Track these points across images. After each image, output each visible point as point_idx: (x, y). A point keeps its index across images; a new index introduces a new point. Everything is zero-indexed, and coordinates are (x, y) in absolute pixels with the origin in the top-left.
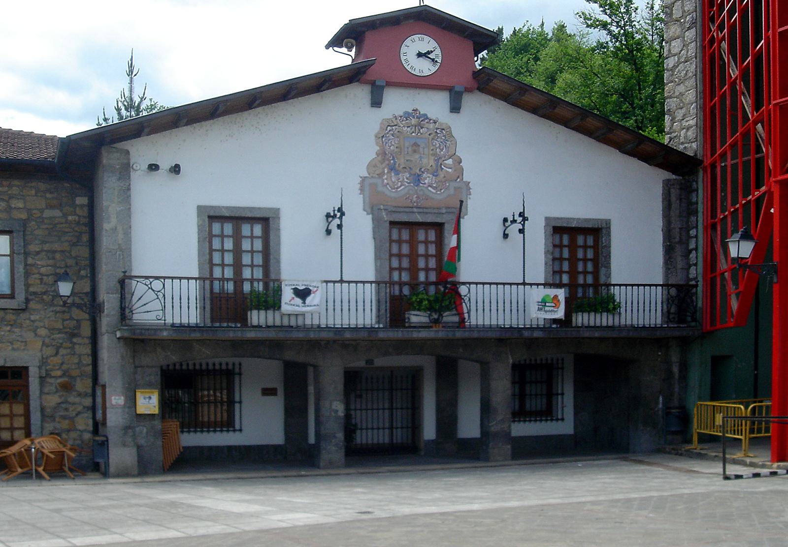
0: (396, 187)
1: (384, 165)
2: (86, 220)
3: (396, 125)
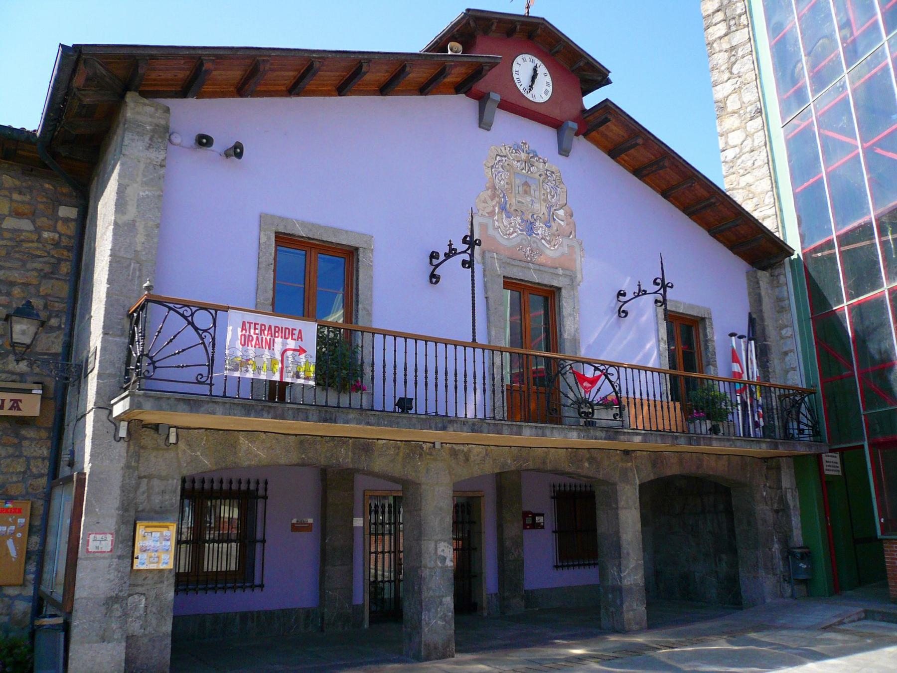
0: (508, 232)
1: (494, 203)
2: (73, 242)
3: (505, 156)
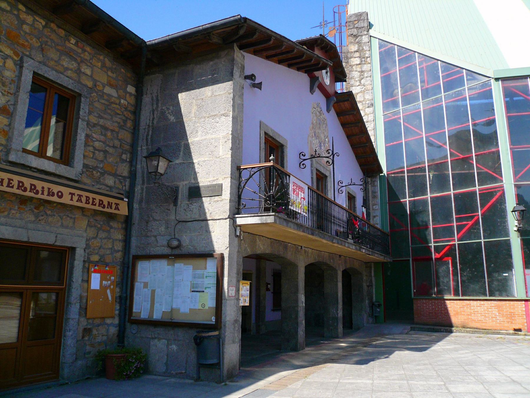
2: (132, 109)
